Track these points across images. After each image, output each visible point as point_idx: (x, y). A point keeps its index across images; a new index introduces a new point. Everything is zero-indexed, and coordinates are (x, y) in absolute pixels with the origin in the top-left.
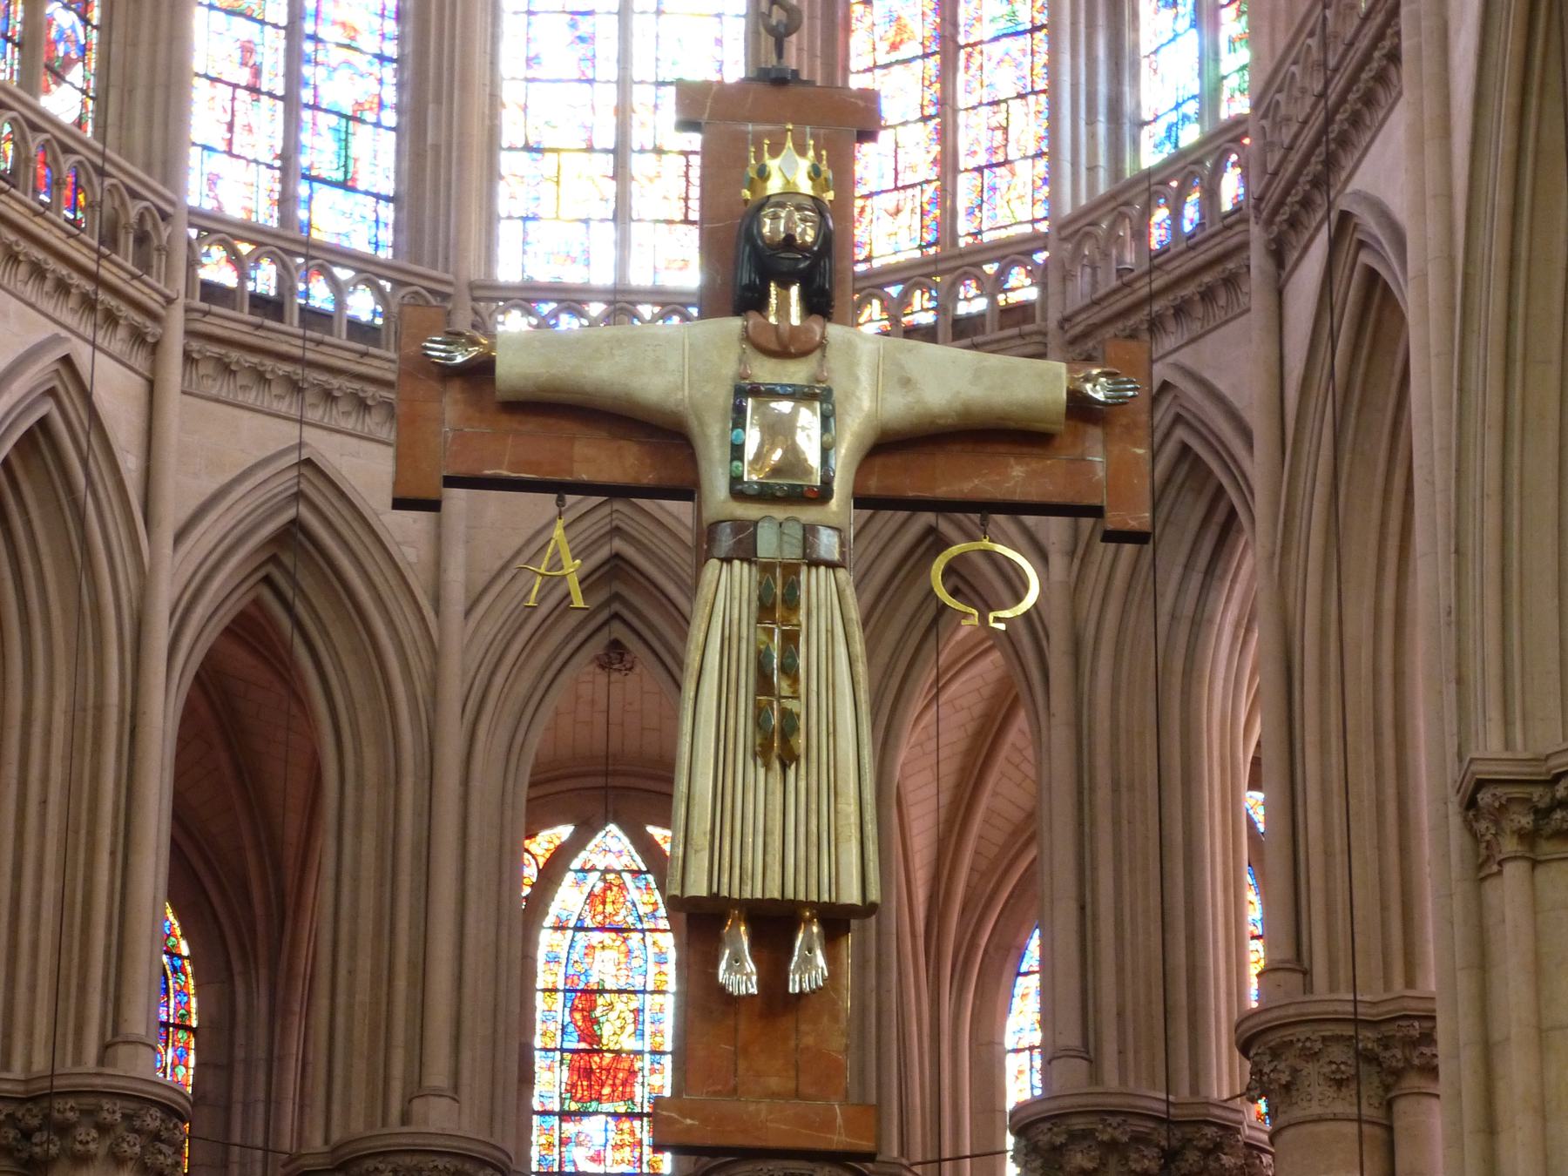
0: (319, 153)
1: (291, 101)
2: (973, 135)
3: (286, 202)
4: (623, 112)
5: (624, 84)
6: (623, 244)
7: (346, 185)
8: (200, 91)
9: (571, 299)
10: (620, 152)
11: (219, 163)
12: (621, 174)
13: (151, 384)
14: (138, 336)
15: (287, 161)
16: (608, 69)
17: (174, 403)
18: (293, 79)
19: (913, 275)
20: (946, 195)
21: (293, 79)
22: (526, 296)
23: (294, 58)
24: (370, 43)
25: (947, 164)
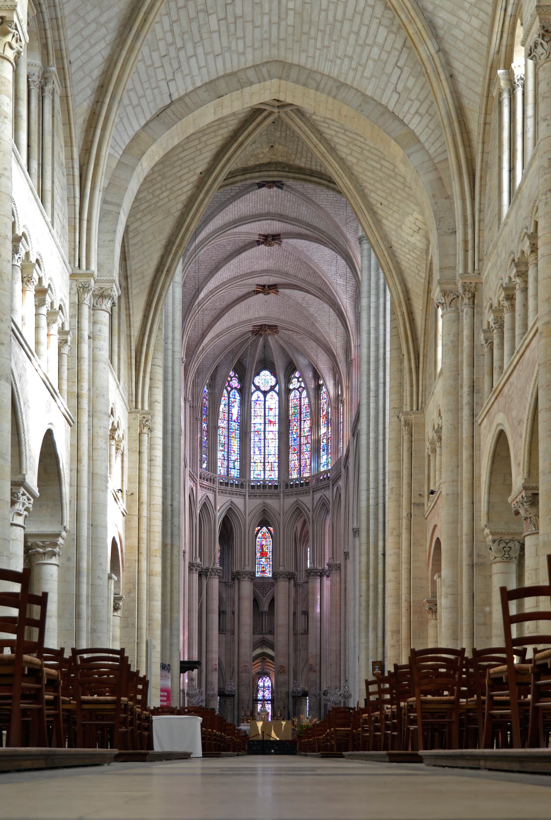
0: (231, 465)
1: (228, 460)
2: (303, 462)
3: (228, 472)
4: (264, 458)
5: (265, 455)
6: (264, 473)
7: (234, 468)
8: (219, 460)
9: (259, 481)
10: (264, 463)
11: (221, 468)
12: (264, 465)
13: (215, 495)
14: (213, 490)
15: (228, 467)
16: (263, 453)
17: (218, 497)
18: (228, 458)
19: (297, 479)
20: (300, 469)
21: (228, 458)
22: (253, 481)
23: (228, 455)
24: (236, 452)
25: (300, 465)
